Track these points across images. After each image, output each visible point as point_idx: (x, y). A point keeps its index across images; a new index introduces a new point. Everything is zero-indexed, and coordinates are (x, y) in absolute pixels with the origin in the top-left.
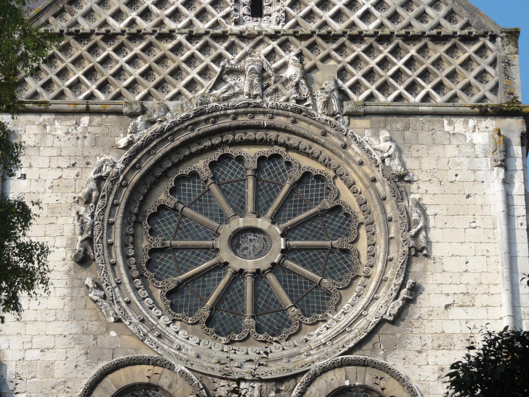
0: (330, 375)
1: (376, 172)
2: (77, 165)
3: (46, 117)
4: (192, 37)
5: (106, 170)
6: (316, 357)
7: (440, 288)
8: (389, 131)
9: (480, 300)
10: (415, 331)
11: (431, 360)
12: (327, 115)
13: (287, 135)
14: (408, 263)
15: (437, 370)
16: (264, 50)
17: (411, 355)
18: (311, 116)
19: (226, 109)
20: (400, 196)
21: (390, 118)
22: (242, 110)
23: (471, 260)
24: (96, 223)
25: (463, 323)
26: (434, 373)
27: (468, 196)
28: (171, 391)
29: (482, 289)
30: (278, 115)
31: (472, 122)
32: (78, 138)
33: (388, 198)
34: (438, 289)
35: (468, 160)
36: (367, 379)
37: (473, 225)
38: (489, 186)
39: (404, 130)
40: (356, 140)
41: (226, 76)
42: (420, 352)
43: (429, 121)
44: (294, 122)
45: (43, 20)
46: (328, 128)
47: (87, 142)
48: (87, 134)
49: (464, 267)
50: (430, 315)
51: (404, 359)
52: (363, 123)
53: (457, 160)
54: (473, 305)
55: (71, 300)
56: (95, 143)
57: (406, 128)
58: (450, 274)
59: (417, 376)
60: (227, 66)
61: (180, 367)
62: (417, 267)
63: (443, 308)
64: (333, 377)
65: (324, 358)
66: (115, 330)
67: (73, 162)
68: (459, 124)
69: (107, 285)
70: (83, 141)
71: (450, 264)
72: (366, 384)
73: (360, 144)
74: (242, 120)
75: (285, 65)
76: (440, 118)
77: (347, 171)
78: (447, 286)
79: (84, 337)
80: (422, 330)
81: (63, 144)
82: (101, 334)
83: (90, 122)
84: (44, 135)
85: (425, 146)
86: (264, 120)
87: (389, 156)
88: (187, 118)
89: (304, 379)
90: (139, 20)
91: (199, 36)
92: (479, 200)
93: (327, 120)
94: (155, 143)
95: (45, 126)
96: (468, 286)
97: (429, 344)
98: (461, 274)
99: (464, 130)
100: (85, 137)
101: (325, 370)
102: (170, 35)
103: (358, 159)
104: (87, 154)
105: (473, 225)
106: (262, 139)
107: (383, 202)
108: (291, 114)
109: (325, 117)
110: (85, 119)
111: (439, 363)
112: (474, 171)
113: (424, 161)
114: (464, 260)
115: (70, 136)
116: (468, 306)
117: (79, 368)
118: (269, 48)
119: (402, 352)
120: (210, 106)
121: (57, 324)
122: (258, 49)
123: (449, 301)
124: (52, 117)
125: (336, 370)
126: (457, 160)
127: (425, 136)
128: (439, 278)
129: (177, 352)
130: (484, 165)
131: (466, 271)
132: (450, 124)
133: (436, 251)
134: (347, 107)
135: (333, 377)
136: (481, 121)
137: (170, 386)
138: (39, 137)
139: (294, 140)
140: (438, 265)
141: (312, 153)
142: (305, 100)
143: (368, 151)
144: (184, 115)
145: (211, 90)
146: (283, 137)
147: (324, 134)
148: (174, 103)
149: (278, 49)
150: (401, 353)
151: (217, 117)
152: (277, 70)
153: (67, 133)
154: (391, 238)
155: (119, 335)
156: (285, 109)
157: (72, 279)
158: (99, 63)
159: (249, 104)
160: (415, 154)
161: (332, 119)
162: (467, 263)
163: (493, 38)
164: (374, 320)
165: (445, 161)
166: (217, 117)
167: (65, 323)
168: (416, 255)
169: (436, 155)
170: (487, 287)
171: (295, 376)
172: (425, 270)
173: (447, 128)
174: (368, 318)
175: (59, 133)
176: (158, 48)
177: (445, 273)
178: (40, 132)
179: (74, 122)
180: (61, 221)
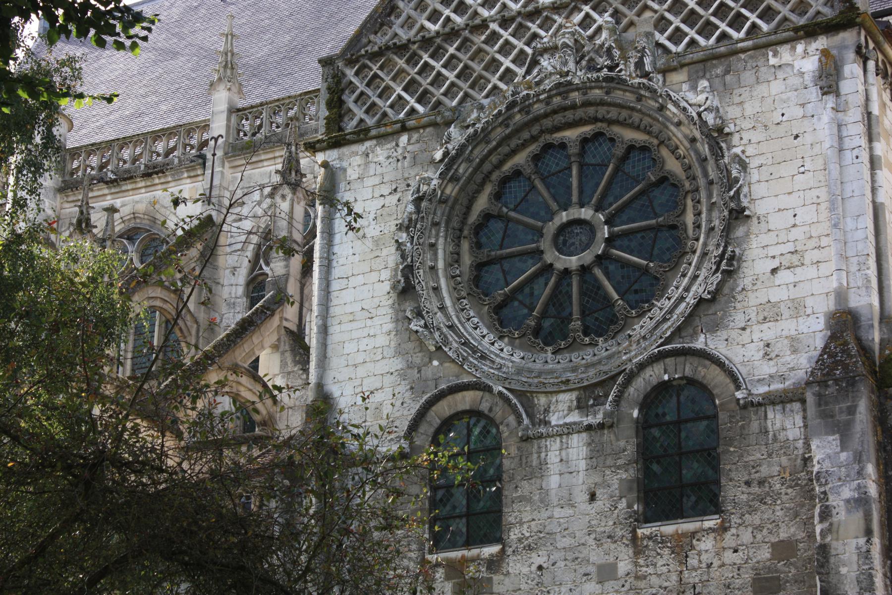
1: (694, 131)
2: (398, 190)
3: (368, 144)
4: (505, 23)
5: (424, 188)
6: (633, 353)
7: (765, 251)
8: (708, 80)
9: (811, 256)
10: (738, 305)
11: (756, 337)
12: (641, 77)
13: (605, 108)
14: (728, 230)
15: (762, 347)
17: (734, 334)
18: (622, 82)
19: (538, 95)
20: (717, 152)
21: (709, 64)
22: (554, 92)
23: (798, 212)
24: (416, 247)
25: (791, 286)
26: (759, 350)
27: (796, 137)
28: (491, 415)
29: (812, 243)
30: (591, 88)
31: (800, 48)
32: (398, 160)
33: (708, 158)
34: (762, 253)
35: (796, 93)
36: (687, 369)
37: (802, 169)
38: (819, 119)
39: (725, 75)
40: (671, 99)
41: (539, 58)
42: (744, 329)
43: (751, 57)
44: (607, 93)
45: (365, 40)
46: (643, 92)
47: (406, 163)
48: (406, 155)
49: (792, 221)
50: (754, 285)
51: (727, 340)
53: (784, 96)
54: (803, 264)
55: (396, 335)
56: (415, 162)
57: (727, 72)
58: (776, 233)
59: (741, 357)
60: (539, 46)
62: (740, 232)
63: (769, 274)
64: (652, 373)
65: (641, 354)
66: (437, 359)
67: (394, 187)
68: (785, 54)
69: (428, 312)
70: (403, 163)
71: (777, 222)
72: (686, 375)
73: (676, 104)
75: (599, 29)
76: (764, 50)
77: (669, 136)
78: (773, 247)
79: (409, 371)
80: (745, 304)
81: (384, 170)
82: (424, 366)
83: (409, 140)
84: (367, 164)
85: (748, 88)
86: (575, 96)
87: (705, 110)
88: (500, 112)
89: (620, 379)
90: (453, 16)
91: (513, 19)
92: (808, 139)
93: (639, 83)
94: (470, 148)
95: (367, 155)
96: (796, 243)
97: (754, 319)
98: (788, 230)
99: (791, 59)
100: (405, 158)
101: (642, 366)
102: (484, 25)
103: (676, 120)
104: (406, 175)
105: (802, 169)
106: (581, 119)
107: (704, 164)
108: (604, 84)
109: (638, 80)
110: (404, 139)
111: (764, 339)
112: (803, 105)
113: (746, 106)
114: (791, 213)
115: (391, 160)
116: (797, 266)
117: (405, 405)
118: (582, 14)
119: (725, 333)
120: (521, 95)
121: (385, 361)
122: (571, 18)
123: (775, 264)
124: (374, 142)
125: (655, 365)
126: (784, 96)
127: (748, 76)
128: (764, 239)
129: (496, 373)
130: (815, 95)
131: (794, 226)
132: (775, 55)
133: (759, 208)
134: (660, 63)
135: (652, 373)
136: (810, 43)
137: (491, 410)
138: (362, 167)
139: (613, 113)
140: (763, 224)
141: (633, 123)
142: (617, 65)
143: (684, 109)
144: (495, 112)
145: (524, 77)
146: (602, 111)
147: (640, 99)
148: (488, 100)
149: (592, 13)
150: (723, 334)
151: (530, 105)
152: (591, 38)
153: (388, 157)
154: (714, 203)
155: (441, 364)
156: (597, 80)
157: (397, 312)
158: (416, 73)
159: (560, 84)
160: (737, 100)
161: (645, 81)
162: (795, 216)
164: (692, 302)
165: (770, 100)
166: (530, 105)
167: (392, 359)
168: (736, 218)
169: (760, 96)
170: (817, 240)
171: (614, 378)
172: (747, 234)
173: (773, 61)
174: (687, 300)
175: (381, 159)
176: (472, 42)
177: (771, 233)
178: (363, 162)
179: (394, 144)
180: (385, 252)
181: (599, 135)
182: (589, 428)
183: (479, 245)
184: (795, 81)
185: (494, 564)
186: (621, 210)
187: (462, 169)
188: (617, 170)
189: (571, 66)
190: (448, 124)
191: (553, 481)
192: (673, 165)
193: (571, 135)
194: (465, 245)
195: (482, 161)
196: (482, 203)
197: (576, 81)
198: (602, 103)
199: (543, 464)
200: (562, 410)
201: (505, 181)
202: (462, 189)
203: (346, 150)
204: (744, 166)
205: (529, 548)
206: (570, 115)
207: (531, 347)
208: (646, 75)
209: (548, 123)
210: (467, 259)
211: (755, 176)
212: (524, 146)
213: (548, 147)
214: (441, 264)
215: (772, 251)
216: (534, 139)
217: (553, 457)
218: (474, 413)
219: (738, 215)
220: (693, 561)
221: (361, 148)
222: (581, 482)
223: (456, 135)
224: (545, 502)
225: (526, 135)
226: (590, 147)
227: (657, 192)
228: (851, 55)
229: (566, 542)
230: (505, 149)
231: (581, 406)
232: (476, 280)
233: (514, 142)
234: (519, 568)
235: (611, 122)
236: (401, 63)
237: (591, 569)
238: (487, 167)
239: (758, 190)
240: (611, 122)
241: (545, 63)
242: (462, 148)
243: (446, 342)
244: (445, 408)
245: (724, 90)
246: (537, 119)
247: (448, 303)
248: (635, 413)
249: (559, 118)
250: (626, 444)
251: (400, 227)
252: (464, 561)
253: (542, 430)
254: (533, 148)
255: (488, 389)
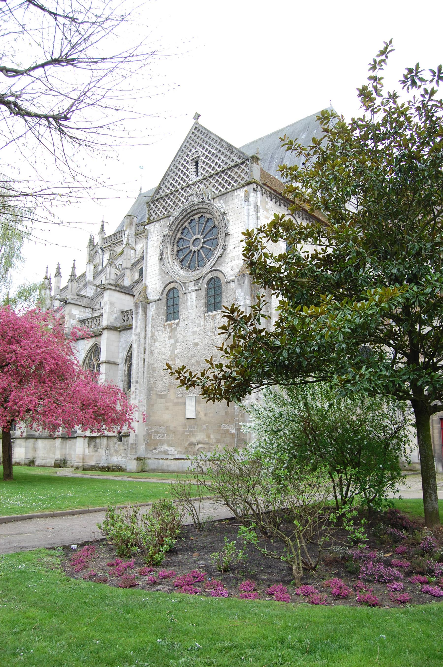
0: (208, 275)
4: (182, 189)
16: (197, 186)
18: (205, 202)
20: (223, 218)
31: (242, 190)
52: (216, 200)
61: (178, 282)
62: (227, 238)
74: (192, 209)
86: (196, 207)
92: (242, 214)
101: (207, 274)
110: (162, 221)
127: (231, 198)
134: (213, 197)
146: (202, 210)
150: (223, 265)
163: (248, 160)
181: (202, 216)
182: (196, 290)
183: (178, 246)
184: (240, 199)
185: (177, 324)
186: (206, 235)
187: (174, 228)
188: (206, 225)
189: (195, 199)
190: (170, 216)
191: (189, 304)
192: (216, 223)
193: (196, 217)
194: (175, 246)
195: (178, 225)
196: (179, 236)
197: (196, 203)
198: (201, 208)
199: (187, 299)
200: (191, 287)
201: (183, 229)
202: (174, 233)
203: (150, 225)
204: (229, 221)
205: (184, 320)
206: (196, 212)
207: (188, 271)
208: (209, 200)
209: (191, 214)
210: (175, 250)
211: (231, 223)
212: (187, 220)
213: (192, 220)
214: (169, 252)
215: (234, 243)
216: (189, 218)
217: (189, 298)
218: (174, 288)
219: (227, 234)
220: (215, 321)
221: (153, 224)
222: (194, 303)
223: (172, 219)
224: (187, 309)
225: (187, 217)
226: (201, 219)
227: (214, 229)
228: (252, 191)
229: (191, 318)
230: (183, 222)
231: (195, 285)
232: (177, 255)
233: (185, 219)
234: (182, 324)
235: (204, 213)
236: (162, 201)
237: (196, 324)
238: (179, 226)
239: (232, 227)
240: (204, 213)
241: (189, 198)
242: (173, 222)
243: (169, 271)
244: (169, 287)
245: (226, 202)
246: (189, 213)
247: (170, 261)
248: (205, 286)
249: (193, 213)
250: (203, 293)
251: (161, 243)
252: (172, 324)
253: (187, 291)
254: (189, 221)
255: (177, 282)
